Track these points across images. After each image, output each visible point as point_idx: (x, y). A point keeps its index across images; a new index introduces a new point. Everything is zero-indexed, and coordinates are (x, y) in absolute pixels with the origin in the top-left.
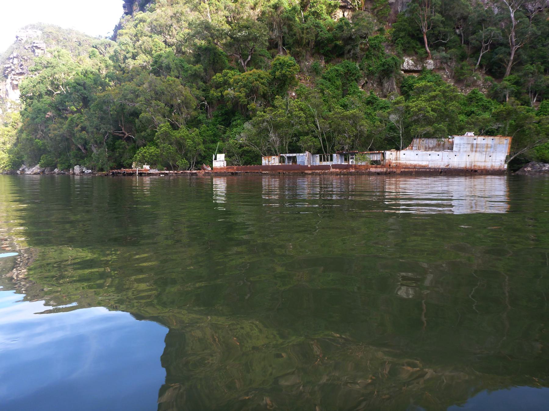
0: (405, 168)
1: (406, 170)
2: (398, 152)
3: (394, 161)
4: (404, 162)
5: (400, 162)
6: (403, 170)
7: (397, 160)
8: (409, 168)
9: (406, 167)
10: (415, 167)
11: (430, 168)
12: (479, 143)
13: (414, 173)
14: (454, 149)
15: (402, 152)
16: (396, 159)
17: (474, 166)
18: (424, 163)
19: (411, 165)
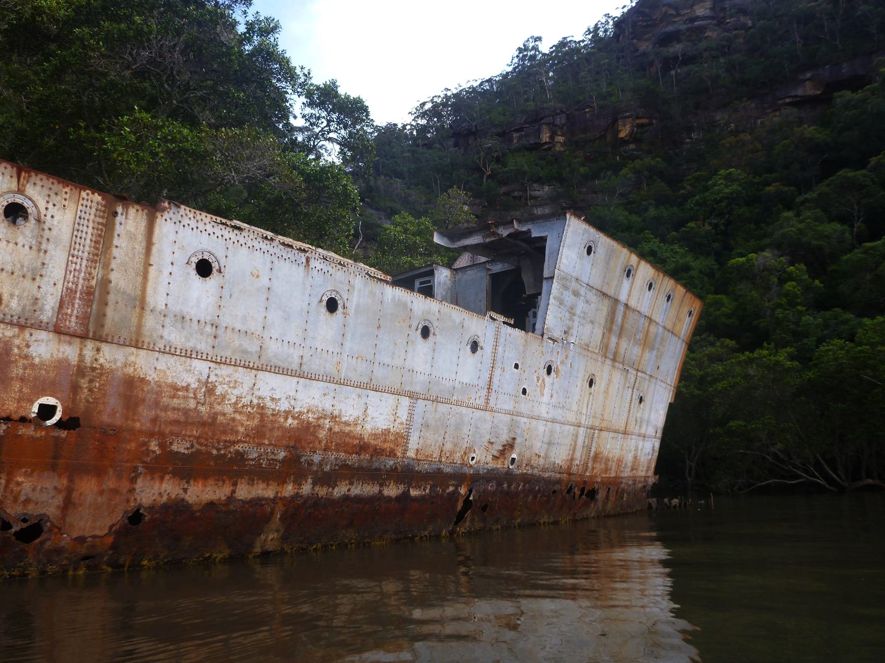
0: (187, 468)
1: (200, 493)
2: (130, 221)
3: (44, 348)
4: (189, 374)
5: (148, 366)
6: (153, 492)
7: (92, 330)
8: (233, 467)
9: (209, 447)
10: (296, 447)
11: (407, 474)
12: (633, 303)
13: (270, 538)
14: (552, 315)
15: (185, 232)
16: (90, 313)
17: (596, 458)
18: (374, 415)
19: (264, 422)
